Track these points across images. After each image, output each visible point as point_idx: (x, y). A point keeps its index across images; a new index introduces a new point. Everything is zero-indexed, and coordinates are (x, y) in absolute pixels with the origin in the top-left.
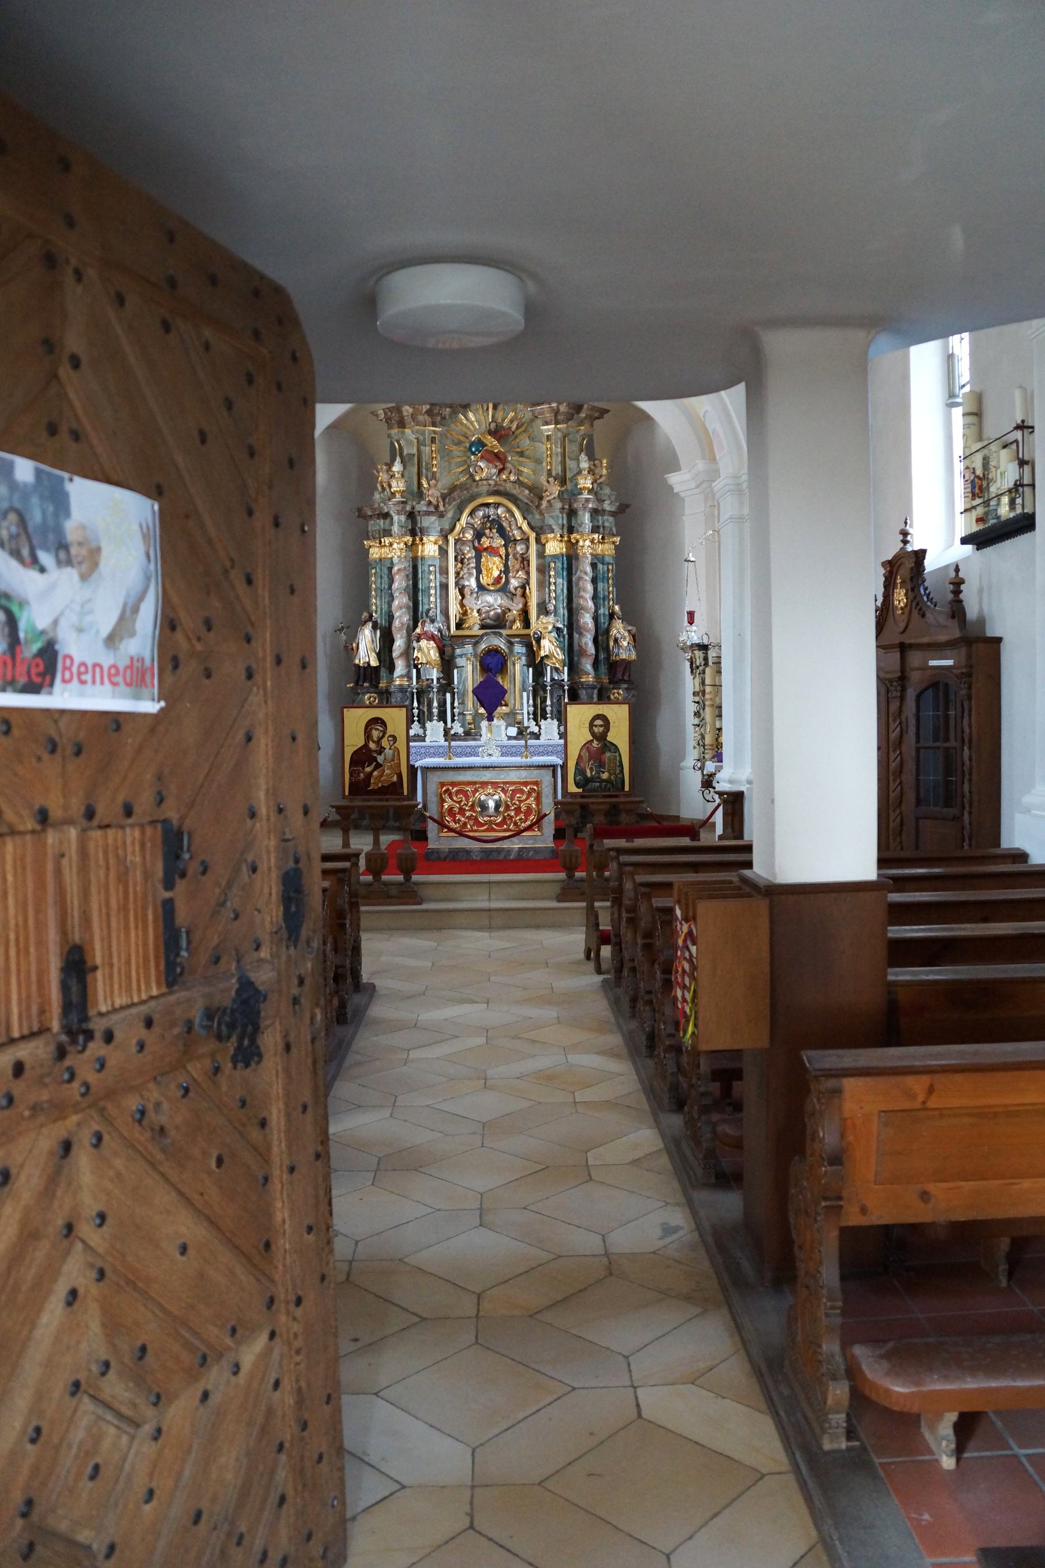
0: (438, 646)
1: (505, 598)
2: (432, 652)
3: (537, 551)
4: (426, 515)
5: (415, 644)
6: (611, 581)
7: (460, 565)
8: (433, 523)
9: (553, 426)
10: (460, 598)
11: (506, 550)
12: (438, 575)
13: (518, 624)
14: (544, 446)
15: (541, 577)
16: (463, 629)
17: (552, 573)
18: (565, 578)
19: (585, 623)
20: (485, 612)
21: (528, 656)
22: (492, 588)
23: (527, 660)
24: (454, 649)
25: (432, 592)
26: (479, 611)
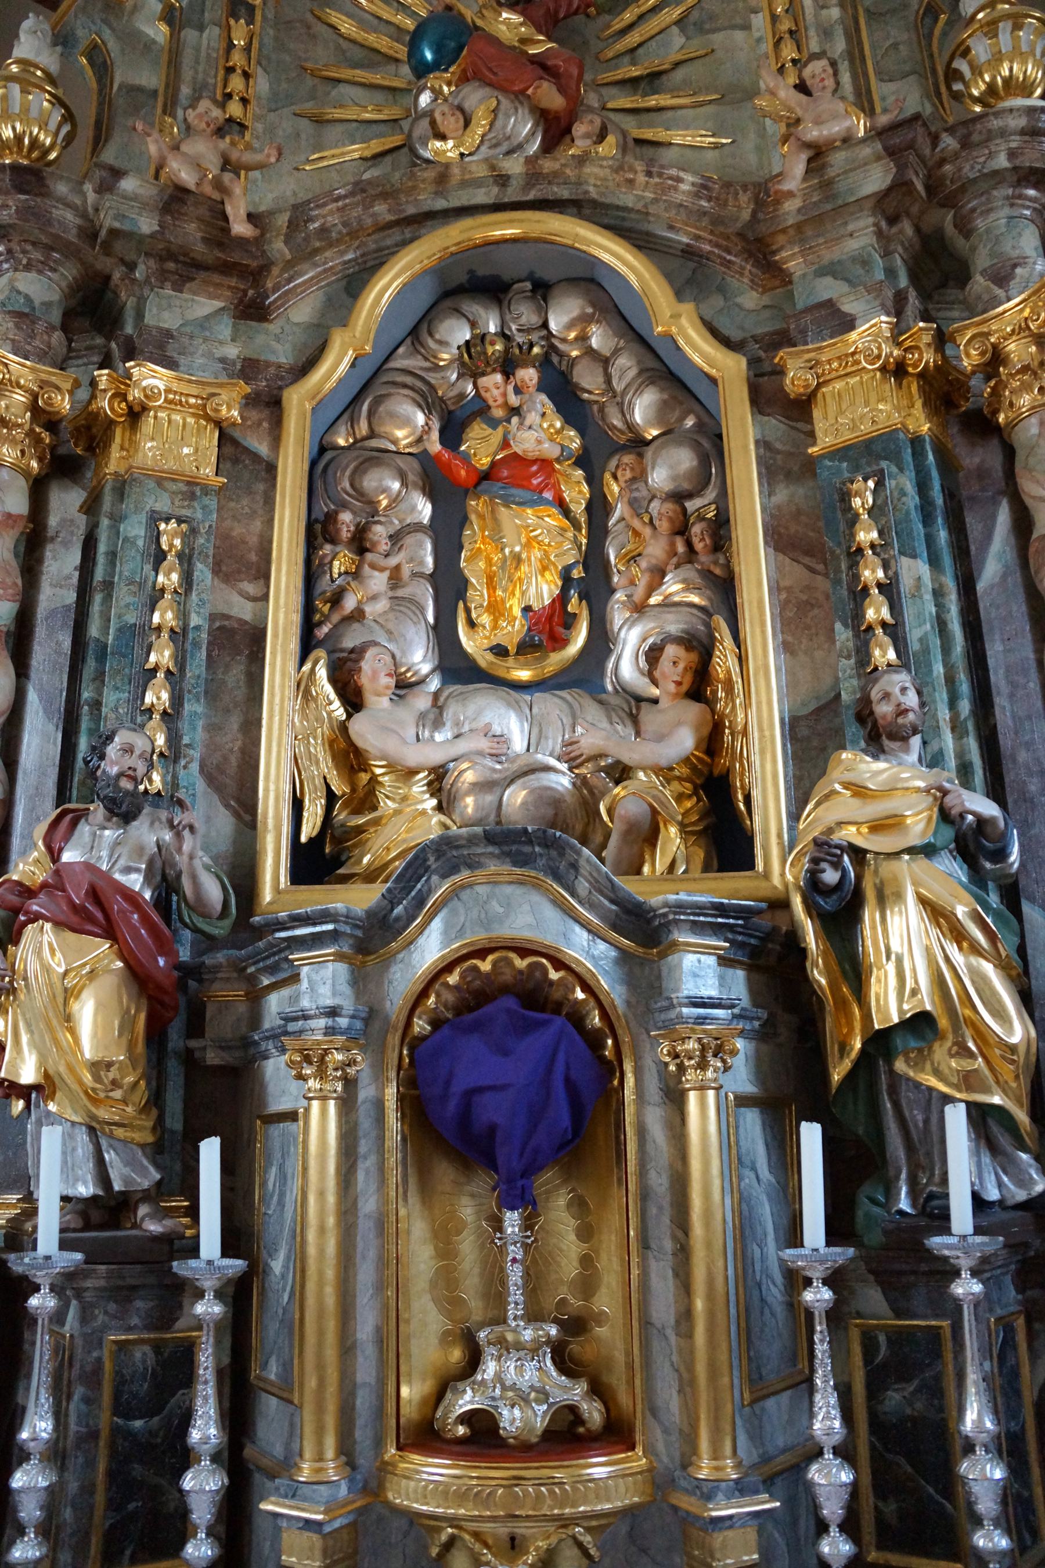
1: (592, 711)
3: (763, 444)
4: (163, 276)
8: (205, 323)
11: (593, 480)
12: (202, 572)
15: (796, 573)
16: (345, 879)
17: (867, 535)
18: (947, 560)
20: (483, 786)
21: (763, 1035)
23: (761, 1070)
24: (256, 997)
25: (162, 656)
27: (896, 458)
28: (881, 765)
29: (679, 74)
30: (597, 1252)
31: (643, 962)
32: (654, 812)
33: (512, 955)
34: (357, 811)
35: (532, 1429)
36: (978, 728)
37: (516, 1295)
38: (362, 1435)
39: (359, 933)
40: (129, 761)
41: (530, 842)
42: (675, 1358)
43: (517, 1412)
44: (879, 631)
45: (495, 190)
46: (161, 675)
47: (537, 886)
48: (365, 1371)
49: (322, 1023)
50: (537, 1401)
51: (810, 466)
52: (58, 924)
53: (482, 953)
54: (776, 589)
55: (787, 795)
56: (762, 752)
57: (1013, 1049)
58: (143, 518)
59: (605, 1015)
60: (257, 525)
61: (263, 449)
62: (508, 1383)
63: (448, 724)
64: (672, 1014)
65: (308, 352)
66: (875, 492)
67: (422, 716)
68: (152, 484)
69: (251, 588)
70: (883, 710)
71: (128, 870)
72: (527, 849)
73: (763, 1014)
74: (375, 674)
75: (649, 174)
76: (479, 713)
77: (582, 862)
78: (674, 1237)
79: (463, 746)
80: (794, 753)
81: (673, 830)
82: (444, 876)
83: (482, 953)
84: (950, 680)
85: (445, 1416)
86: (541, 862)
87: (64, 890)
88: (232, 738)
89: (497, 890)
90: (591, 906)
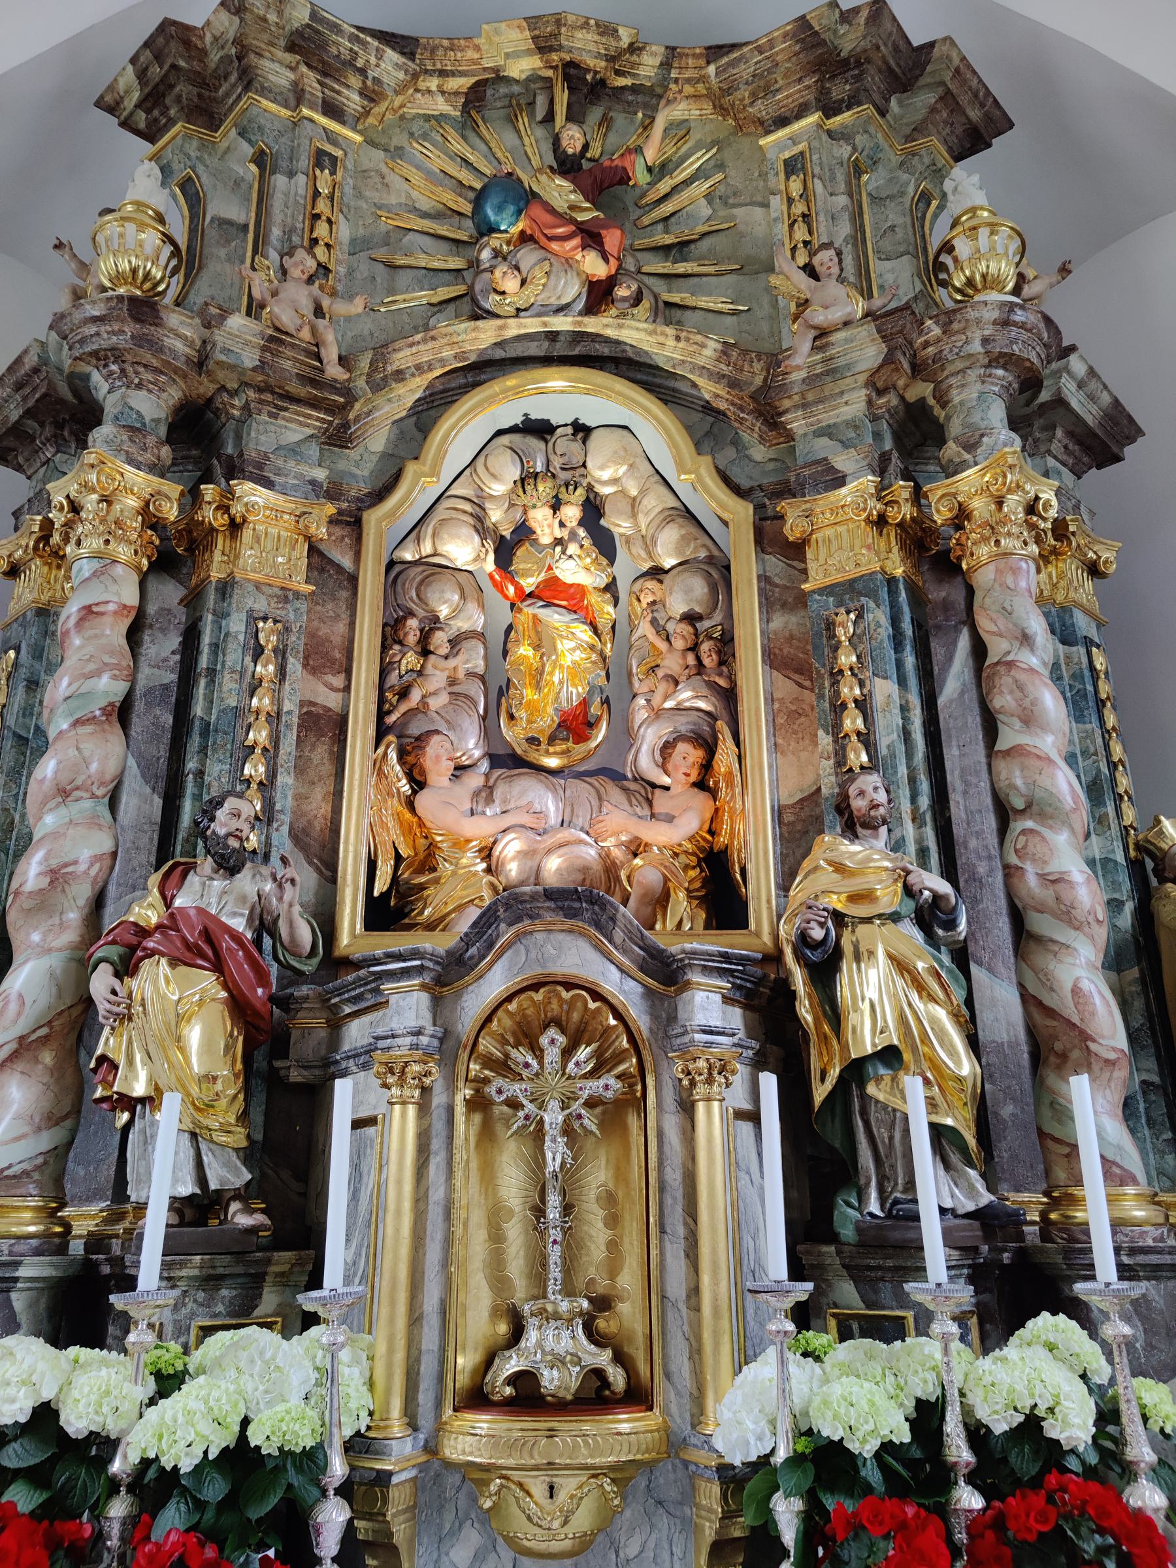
0: (238, 1006)
2: (194, 1035)
5: (101, 983)
6: (1111, 720)
7: (411, 660)
9: (813, 118)
10: (406, 788)
12: (294, 665)
13: (680, 904)
14: (778, 203)
15: (785, 687)
17: (847, 659)
19: (1056, 881)
22: (553, 762)
24: (336, 1024)
25: (260, 735)
26: (487, 853)
27: (873, 595)
28: (855, 848)
29: (705, 244)
30: (621, 1238)
31: (662, 997)
32: (666, 879)
33: (560, 988)
34: (420, 871)
35: (567, 1389)
36: (935, 820)
37: (555, 1272)
38: (425, 1398)
39: (438, 968)
40: (234, 824)
41: (579, 900)
42: (686, 1328)
43: (555, 1373)
44: (854, 738)
45: (546, 344)
46: (258, 751)
47: (583, 934)
48: (430, 1338)
49: (408, 1040)
50: (571, 1362)
51: (802, 600)
52: (174, 962)
53: (535, 987)
54: (770, 699)
55: (776, 869)
56: (756, 834)
57: (960, 1079)
58: (244, 616)
59: (632, 1039)
60: (341, 628)
61: (346, 562)
62: (548, 1349)
63: (497, 801)
64: (686, 1039)
65: (385, 478)
66: (855, 623)
67: (476, 794)
68: (251, 588)
69: (338, 681)
70: (859, 804)
71: (234, 914)
72: (576, 905)
73: (755, 1044)
74: (438, 757)
75: (678, 338)
76: (523, 793)
77: (619, 917)
78: (686, 1224)
79: (509, 820)
80: (781, 835)
81: (682, 895)
82: (510, 925)
83: (535, 987)
84: (912, 780)
85: (494, 1380)
86: (587, 915)
87: (178, 930)
88: (319, 807)
89: (552, 936)
90: (624, 951)
